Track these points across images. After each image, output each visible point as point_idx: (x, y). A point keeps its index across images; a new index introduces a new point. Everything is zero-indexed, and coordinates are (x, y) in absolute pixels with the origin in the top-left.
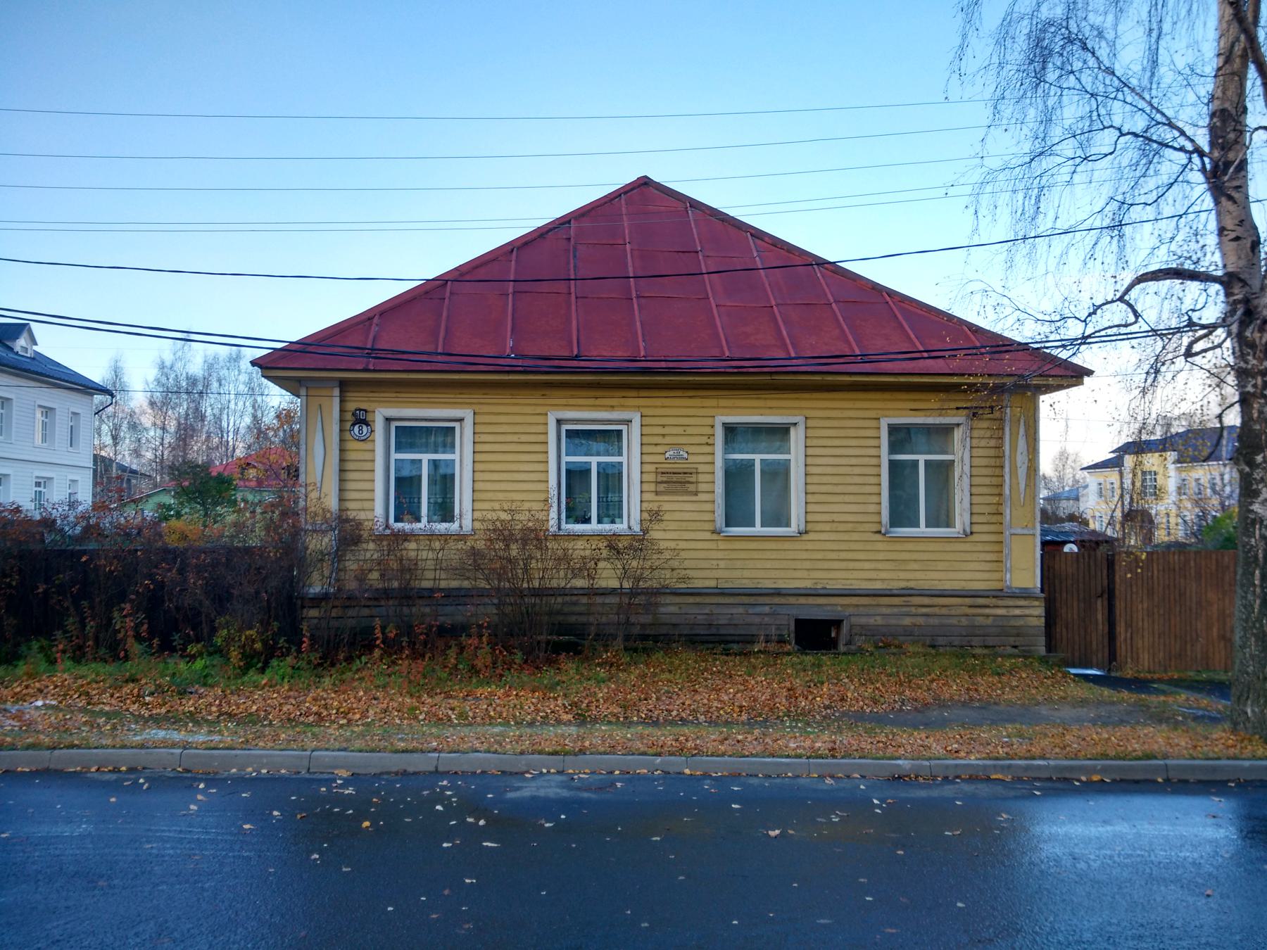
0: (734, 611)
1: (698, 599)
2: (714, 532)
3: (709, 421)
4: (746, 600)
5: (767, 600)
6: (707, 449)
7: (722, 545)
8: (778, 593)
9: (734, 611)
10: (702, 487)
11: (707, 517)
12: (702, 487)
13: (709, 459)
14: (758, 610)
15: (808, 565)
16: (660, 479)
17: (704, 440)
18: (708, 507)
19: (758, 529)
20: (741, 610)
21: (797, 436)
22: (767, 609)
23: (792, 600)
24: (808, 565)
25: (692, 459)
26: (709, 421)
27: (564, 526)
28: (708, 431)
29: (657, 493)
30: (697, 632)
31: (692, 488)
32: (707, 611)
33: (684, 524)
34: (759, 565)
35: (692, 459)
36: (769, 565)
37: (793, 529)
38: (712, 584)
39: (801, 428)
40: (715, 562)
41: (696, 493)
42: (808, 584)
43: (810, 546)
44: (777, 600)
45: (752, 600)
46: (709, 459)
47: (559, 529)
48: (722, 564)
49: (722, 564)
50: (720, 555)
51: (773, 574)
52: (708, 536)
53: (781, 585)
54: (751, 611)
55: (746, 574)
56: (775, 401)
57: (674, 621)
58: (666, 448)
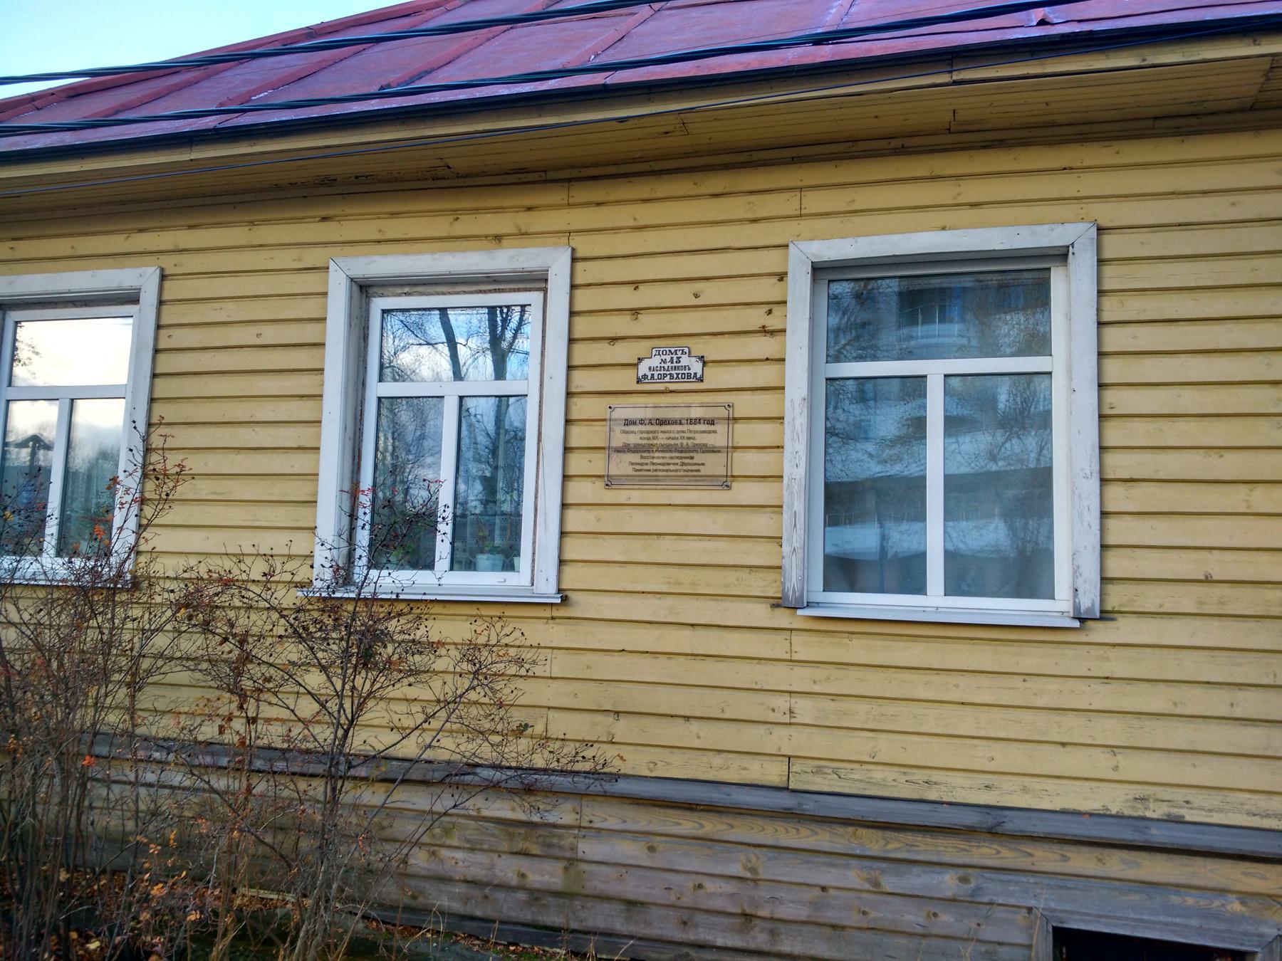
0: (830, 876)
1: (711, 826)
2: (778, 603)
3: (769, 261)
4: (873, 843)
5: (948, 849)
6: (763, 347)
7: (805, 648)
8: (993, 825)
9: (830, 876)
10: (745, 463)
11: (759, 555)
12: (745, 463)
13: (765, 375)
14: (916, 881)
15: (1111, 730)
16: (619, 440)
17: (755, 318)
18: (760, 524)
19: (935, 601)
20: (853, 876)
21: (1071, 293)
22: (948, 883)
23: (1045, 858)
24: (1111, 730)
25: (716, 378)
26: (769, 261)
27: (359, 571)
28: (766, 290)
29: (610, 482)
30: (703, 935)
31: (713, 465)
32: (737, 869)
33: (686, 576)
34: (932, 720)
35: (716, 378)
36: (967, 723)
37: (1054, 608)
38: (773, 773)
39: (1083, 264)
40: (781, 702)
41: (726, 482)
42: (1114, 800)
43: (1119, 665)
44: (984, 853)
45: (895, 845)
46: (765, 375)
47: (348, 581)
48: (806, 710)
49: (806, 710)
50: (800, 679)
51: (979, 756)
52: (760, 614)
53: (1009, 795)
54: (890, 882)
55: (888, 748)
56: (983, 176)
57: (632, 888)
58: (642, 348)
